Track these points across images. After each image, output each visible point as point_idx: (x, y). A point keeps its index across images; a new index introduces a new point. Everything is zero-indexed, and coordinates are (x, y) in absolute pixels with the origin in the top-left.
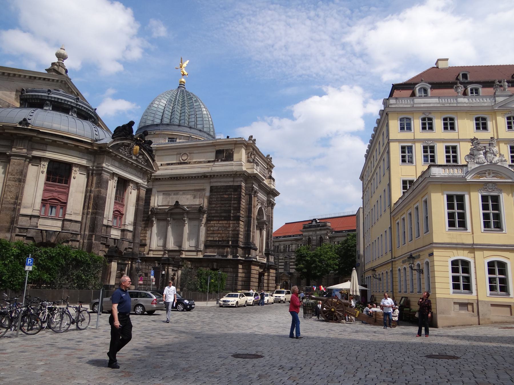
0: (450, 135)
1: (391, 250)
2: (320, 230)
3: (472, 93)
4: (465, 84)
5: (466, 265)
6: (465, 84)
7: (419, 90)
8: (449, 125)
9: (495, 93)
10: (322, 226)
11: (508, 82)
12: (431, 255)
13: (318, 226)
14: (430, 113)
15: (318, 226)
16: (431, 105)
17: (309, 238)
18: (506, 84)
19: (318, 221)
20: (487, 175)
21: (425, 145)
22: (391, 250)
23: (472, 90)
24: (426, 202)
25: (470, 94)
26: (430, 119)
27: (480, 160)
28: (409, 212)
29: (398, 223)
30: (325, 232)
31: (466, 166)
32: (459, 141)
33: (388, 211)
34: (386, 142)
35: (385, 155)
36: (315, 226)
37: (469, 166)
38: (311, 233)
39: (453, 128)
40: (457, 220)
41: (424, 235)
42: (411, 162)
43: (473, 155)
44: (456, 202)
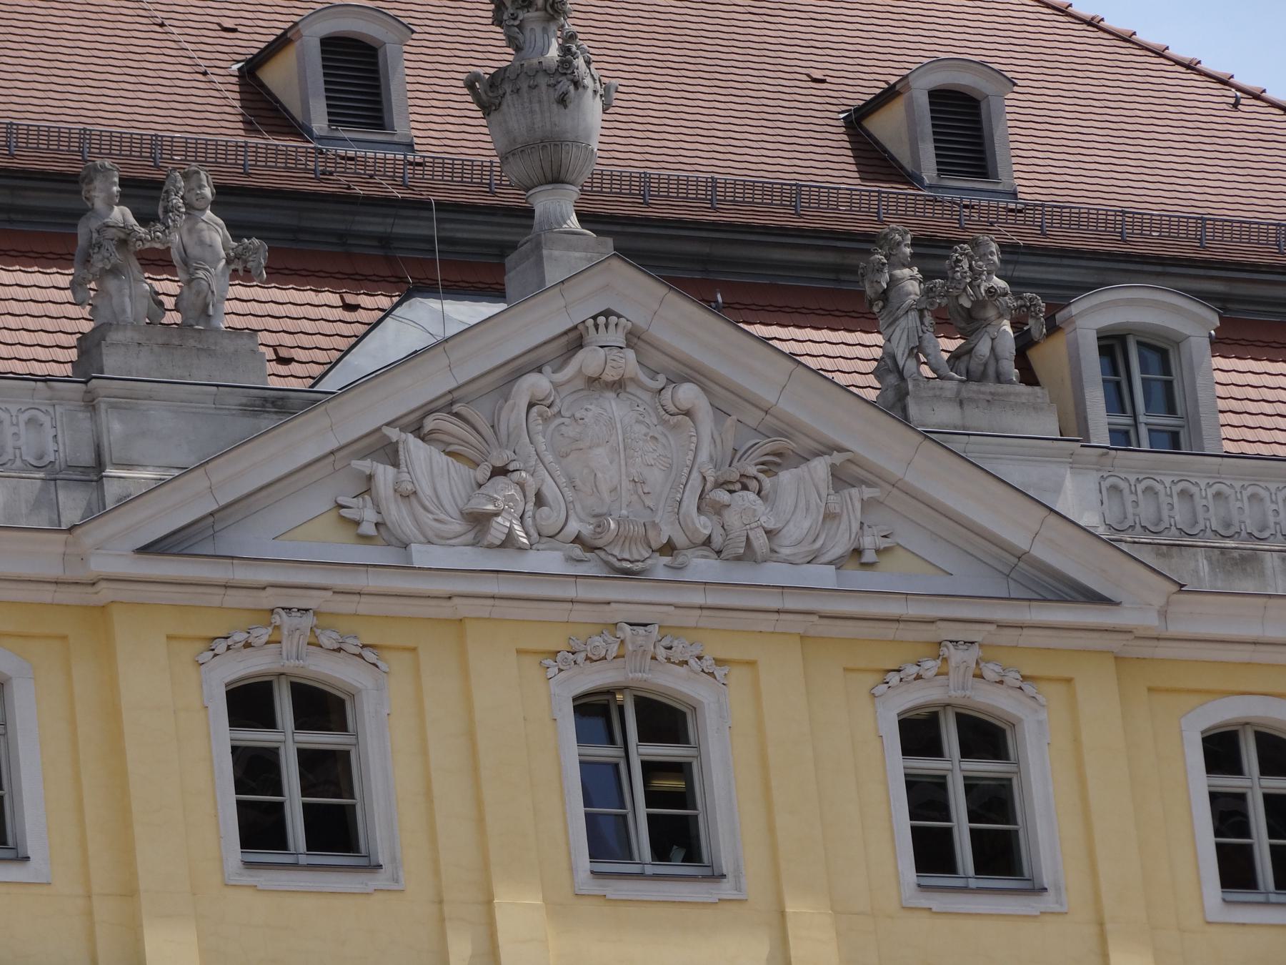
9: (89, 347)
11: (229, 198)
18: (213, 229)
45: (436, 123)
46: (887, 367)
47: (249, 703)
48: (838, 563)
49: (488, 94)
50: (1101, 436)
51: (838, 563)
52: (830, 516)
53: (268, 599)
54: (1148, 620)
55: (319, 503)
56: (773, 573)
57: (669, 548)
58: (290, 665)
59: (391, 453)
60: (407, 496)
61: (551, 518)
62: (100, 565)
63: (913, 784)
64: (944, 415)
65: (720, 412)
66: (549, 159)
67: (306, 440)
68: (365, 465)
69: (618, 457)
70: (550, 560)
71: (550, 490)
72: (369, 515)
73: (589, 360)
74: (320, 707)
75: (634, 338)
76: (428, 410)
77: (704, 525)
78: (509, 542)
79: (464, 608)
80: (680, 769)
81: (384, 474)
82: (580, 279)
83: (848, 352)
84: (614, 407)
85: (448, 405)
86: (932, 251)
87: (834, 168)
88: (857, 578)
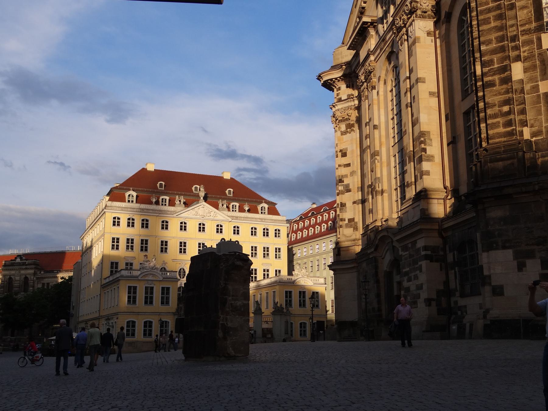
1: (99, 311)
2: (26, 269)
3: (162, 202)
5: (134, 322)
7: (129, 195)
10: (29, 264)
12: (117, 318)
13: (24, 264)
15: (24, 264)
17: (10, 278)
19: (24, 258)
22: (99, 311)
30: (32, 271)
36: (19, 264)
38: (13, 272)
40: (132, 300)
44: (132, 291)
74: (185, 223)
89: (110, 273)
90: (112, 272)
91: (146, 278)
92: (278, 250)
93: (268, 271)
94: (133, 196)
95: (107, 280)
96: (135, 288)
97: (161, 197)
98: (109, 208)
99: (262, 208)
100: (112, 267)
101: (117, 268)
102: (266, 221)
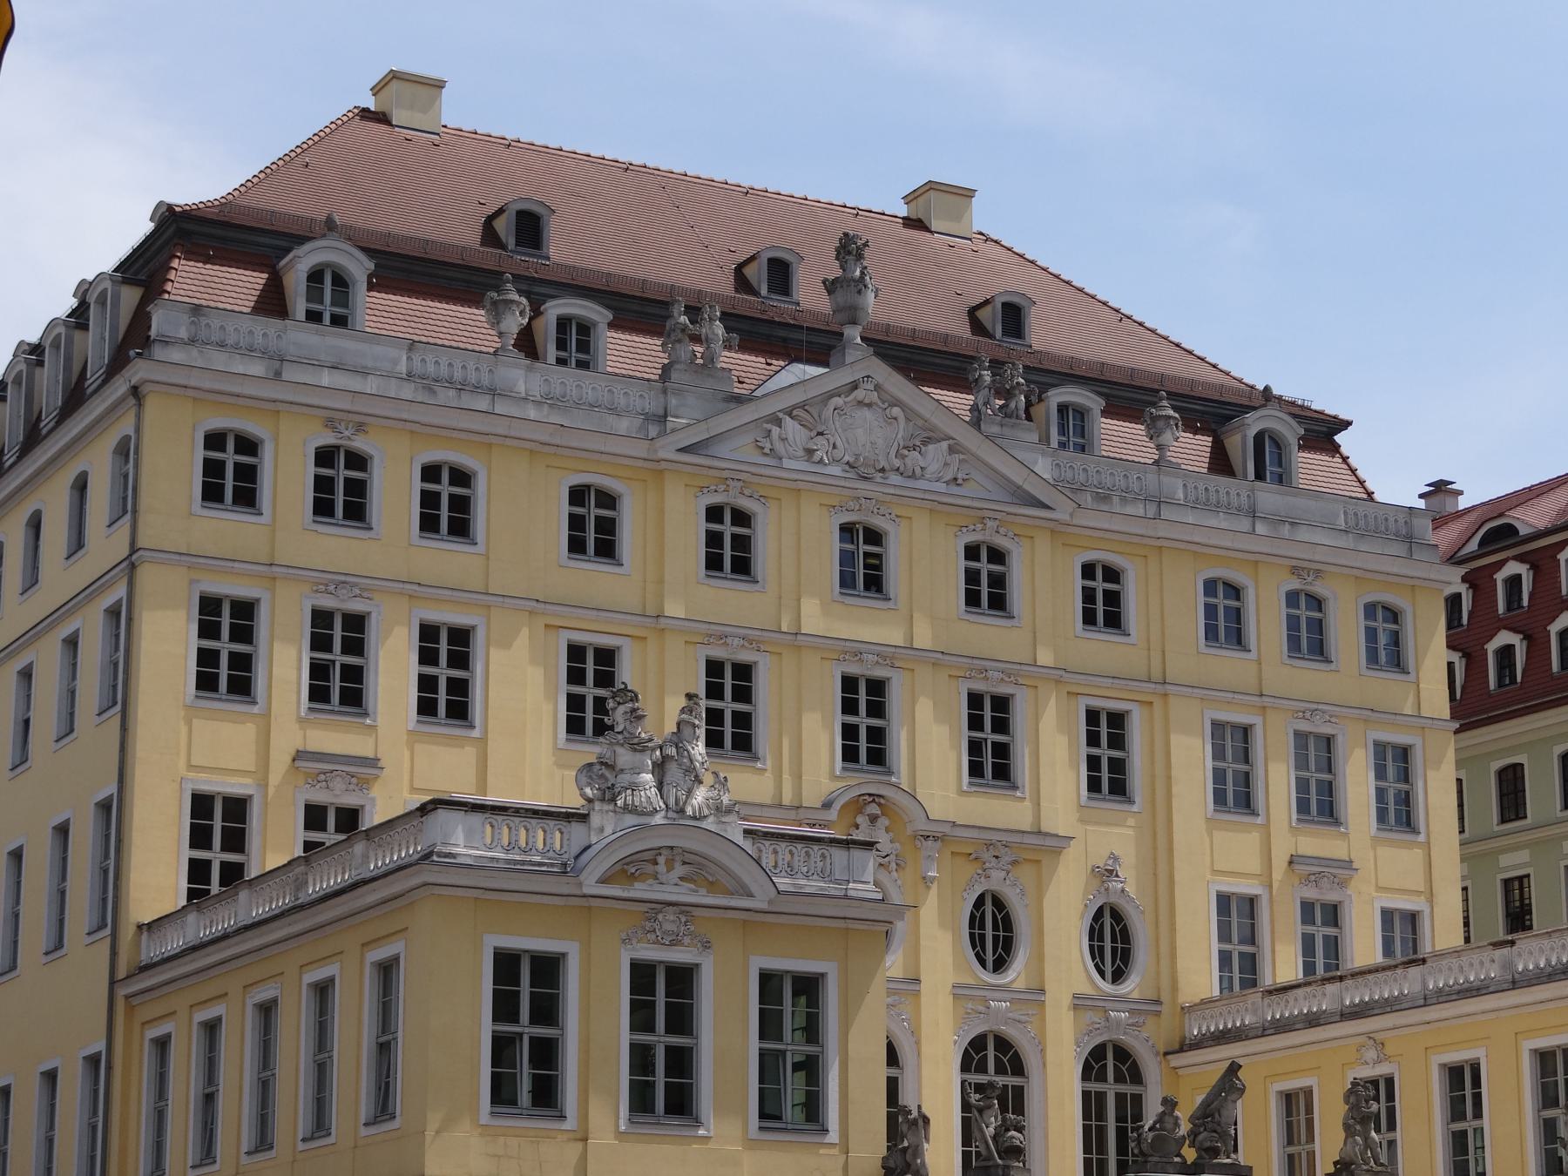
0: (443, 559)
3: (562, 344)
4: (538, 290)
6: (538, 290)
7: (315, 276)
8: (448, 508)
9: (666, 369)
11: (725, 317)
14: (360, 428)
16: (371, 385)
18: (719, 328)
20: (661, 868)
21: (327, 603)
23: (563, 323)
24: (387, 970)
25: (552, 353)
26: (358, 461)
27: (640, 799)
28: (263, 995)
29: (162, 1044)
31: (584, 818)
32: (486, 597)
33: (87, 962)
34: (106, 545)
35: (91, 625)
37: (595, 820)
39: (461, 529)
41: (364, 1131)
42: (242, 687)
43: (611, 767)
44: (527, 990)
45: (810, 296)
46: (974, 409)
47: (714, 514)
48: (947, 483)
49: (831, 286)
50: (1055, 444)
51: (947, 483)
52: (946, 464)
53: (726, 474)
54: (1065, 517)
55: (749, 439)
56: (921, 484)
57: (883, 470)
58: (731, 500)
59: (778, 422)
60: (784, 440)
61: (838, 454)
62: (662, 454)
63: (967, 571)
64: (995, 429)
65: (908, 420)
66: (852, 314)
67: (748, 414)
68: (769, 426)
69: (866, 433)
70: (836, 470)
71: (839, 443)
72: (768, 446)
73: (859, 394)
74: (742, 518)
75: (877, 387)
76: (795, 407)
77: (897, 463)
78: (821, 461)
79: (801, 485)
80: (878, 556)
81: (775, 431)
82: (859, 362)
83: (960, 402)
84: (867, 413)
85: (802, 406)
86: (996, 365)
87: (962, 329)
88: (954, 490)
89: (184, 885)
90: (198, 871)
91: (640, 890)
92: (1396, 763)
93: (1333, 914)
94: (341, 282)
95: (174, 942)
96: (548, 968)
97: (556, 308)
98: (176, 355)
99: (1259, 438)
100: (200, 837)
101: (236, 840)
102: (1304, 534)
